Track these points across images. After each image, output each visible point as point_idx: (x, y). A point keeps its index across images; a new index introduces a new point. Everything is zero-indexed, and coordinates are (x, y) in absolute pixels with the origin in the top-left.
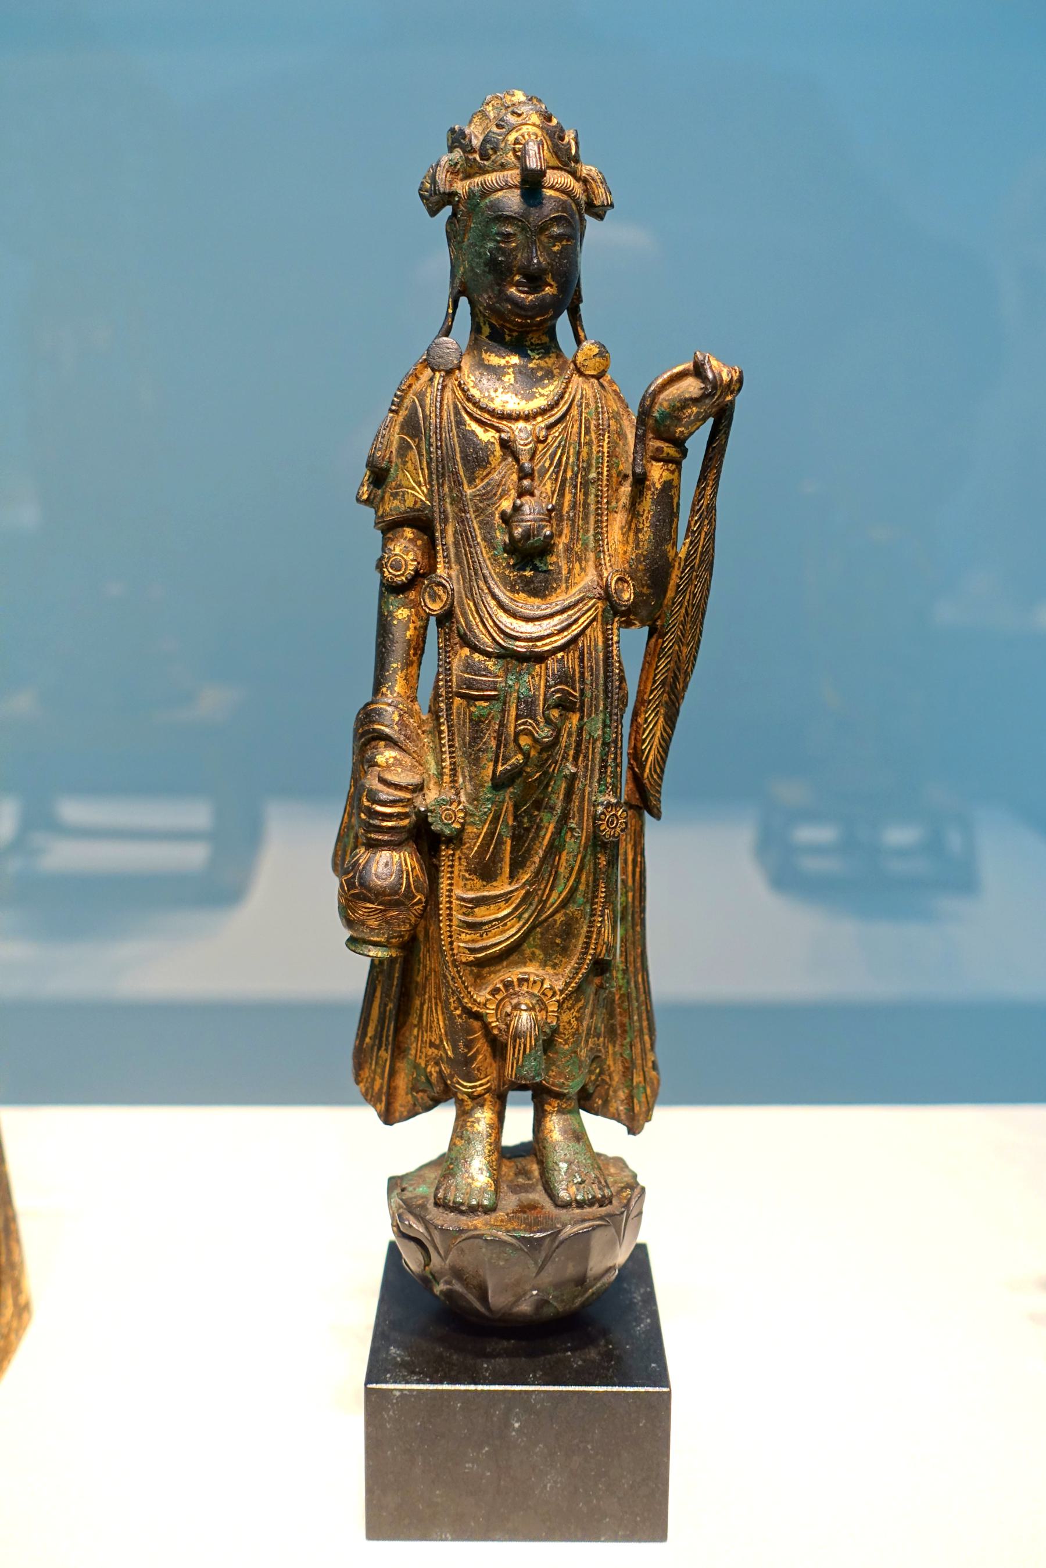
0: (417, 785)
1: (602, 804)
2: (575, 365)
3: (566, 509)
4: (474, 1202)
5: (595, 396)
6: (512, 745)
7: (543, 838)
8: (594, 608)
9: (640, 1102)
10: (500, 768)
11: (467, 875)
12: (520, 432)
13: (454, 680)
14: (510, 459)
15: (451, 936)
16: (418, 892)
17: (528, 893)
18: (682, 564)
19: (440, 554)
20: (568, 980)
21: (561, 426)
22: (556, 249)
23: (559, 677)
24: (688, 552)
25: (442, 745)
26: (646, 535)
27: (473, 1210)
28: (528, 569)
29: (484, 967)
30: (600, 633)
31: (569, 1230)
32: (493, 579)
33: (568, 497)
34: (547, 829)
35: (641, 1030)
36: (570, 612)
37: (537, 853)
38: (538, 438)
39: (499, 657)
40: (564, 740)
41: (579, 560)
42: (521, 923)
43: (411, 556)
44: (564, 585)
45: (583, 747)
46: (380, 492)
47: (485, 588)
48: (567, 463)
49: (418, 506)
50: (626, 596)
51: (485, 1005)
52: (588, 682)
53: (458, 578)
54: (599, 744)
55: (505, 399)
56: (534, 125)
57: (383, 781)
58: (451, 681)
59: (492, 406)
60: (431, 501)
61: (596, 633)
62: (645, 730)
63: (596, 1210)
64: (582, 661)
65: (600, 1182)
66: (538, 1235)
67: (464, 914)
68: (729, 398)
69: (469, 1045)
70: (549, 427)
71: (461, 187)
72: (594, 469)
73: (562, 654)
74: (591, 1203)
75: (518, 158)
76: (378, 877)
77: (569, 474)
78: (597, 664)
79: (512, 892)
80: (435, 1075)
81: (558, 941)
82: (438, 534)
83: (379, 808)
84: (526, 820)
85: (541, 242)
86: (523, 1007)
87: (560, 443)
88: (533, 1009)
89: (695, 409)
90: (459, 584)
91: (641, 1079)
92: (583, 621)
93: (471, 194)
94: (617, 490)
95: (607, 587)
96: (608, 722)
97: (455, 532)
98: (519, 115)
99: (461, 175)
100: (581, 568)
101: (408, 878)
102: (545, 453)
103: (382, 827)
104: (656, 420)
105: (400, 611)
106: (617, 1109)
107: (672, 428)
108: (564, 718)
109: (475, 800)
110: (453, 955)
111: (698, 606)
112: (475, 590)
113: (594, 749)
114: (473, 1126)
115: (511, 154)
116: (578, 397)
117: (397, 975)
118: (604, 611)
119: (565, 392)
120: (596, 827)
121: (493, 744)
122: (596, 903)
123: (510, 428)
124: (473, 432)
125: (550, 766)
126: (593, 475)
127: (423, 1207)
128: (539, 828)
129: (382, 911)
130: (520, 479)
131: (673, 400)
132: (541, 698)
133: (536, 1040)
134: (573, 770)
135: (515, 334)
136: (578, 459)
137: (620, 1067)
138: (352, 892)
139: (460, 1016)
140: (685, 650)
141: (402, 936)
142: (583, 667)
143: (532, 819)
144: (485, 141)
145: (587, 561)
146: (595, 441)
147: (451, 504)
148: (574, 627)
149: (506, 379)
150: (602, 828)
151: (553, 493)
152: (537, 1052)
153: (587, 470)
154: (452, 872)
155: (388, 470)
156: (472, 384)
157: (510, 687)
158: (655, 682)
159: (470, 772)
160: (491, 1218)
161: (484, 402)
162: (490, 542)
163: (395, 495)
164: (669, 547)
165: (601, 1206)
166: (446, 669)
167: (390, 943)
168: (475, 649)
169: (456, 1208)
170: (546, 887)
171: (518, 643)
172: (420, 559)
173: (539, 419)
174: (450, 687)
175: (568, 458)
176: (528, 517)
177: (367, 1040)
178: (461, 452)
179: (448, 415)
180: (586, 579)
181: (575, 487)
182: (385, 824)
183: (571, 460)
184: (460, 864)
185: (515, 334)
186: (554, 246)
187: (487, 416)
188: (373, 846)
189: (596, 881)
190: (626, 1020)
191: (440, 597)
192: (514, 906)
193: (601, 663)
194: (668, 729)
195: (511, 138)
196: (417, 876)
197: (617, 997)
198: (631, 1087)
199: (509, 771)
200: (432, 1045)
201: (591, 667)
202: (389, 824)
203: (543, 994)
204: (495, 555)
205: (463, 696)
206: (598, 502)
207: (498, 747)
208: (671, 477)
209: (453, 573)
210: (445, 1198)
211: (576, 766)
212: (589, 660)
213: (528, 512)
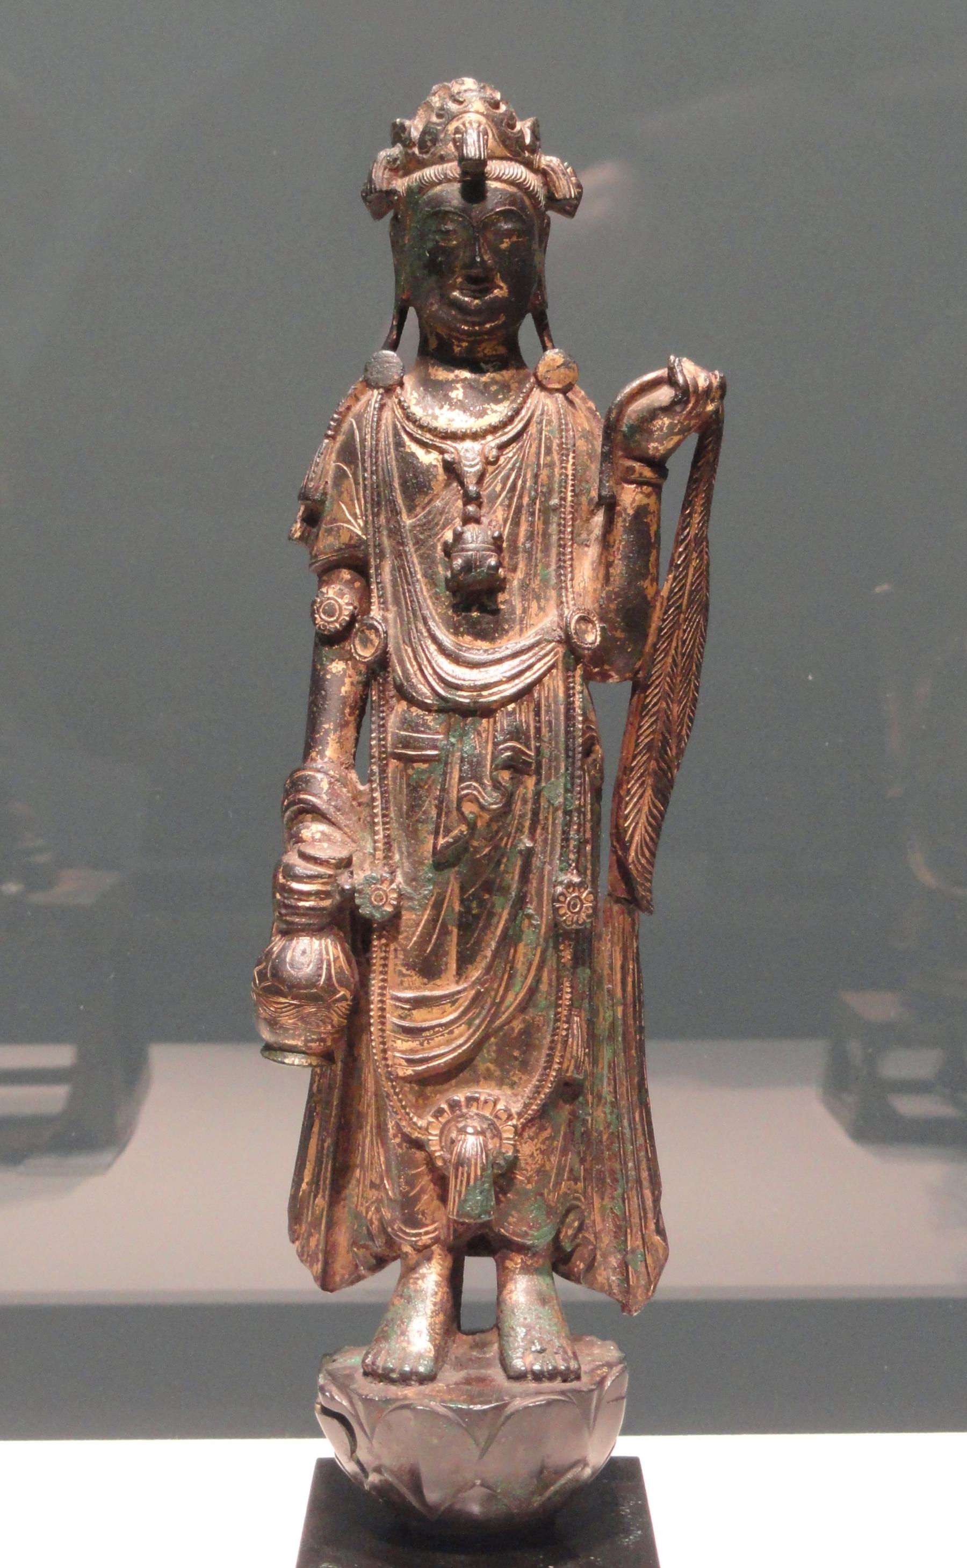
0: (341, 860)
1: (561, 883)
2: (536, 377)
3: (522, 538)
4: (407, 1369)
5: (558, 412)
6: (455, 813)
7: (497, 927)
8: (552, 654)
9: (636, 1271)
10: (441, 841)
11: (404, 971)
12: (469, 454)
13: (389, 738)
14: (455, 484)
15: (384, 1043)
16: (341, 985)
17: (478, 994)
18: (665, 604)
19: (375, 594)
20: (527, 1101)
21: (514, 447)
22: (504, 246)
23: (510, 733)
24: (671, 590)
25: (374, 816)
26: (619, 569)
27: (404, 1379)
28: (474, 608)
29: (429, 1084)
30: (561, 683)
31: (518, 1403)
32: (434, 621)
33: (523, 529)
34: (500, 917)
35: (639, 1181)
36: (524, 657)
37: (489, 945)
38: (487, 458)
39: (440, 711)
40: (518, 808)
41: (538, 598)
42: (471, 1030)
43: (347, 598)
44: (518, 627)
45: (541, 817)
46: (315, 530)
47: (424, 630)
48: (523, 488)
49: (353, 542)
50: (590, 638)
51: (427, 1129)
52: (546, 739)
53: (395, 622)
54: (560, 814)
55: (448, 418)
56: (477, 112)
57: (304, 856)
58: (384, 739)
59: (434, 424)
60: (366, 534)
61: (556, 683)
62: (627, 803)
63: (558, 1385)
64: (538, 714)
65: (565, 1352)
66: (478, 1407)
67: (400, 1017)
68: (710, 408)
69: (411, 1182)
70: (502, 447)
71: (401, 184)
72: (556, 495)
73: (513, 705)
74: (552, 1375)
75: (457, 147)
76: (292, 966)
77: (526, 500)
78: (557, 719)
79: (459, 992)
80: (376, 1223)
81: (516, 1054)
82: (372, 571)
83: (295, 886)
84: (474, 905)
85: (485, 239)
86: (470, 1130)
87: (514, 465)
88: (482, 1133)
89: (667, 421)
90: (396, 627)
91: (639, 1242)
92: (540, 668)
93: (410, 190)
94: (588, 520)
95: (566, 629)
96: (569, 786)
97: (393, 569)
98: (461, 103)
99: (401, 173)
100: (540, 608)
101: (329, 970)
102: (497, 475)
103: (298, 907)
104: (624, 436)
105: (334, 664)
106: (608, 1279)
107: (644, 443)
108: (516, 782)
109: (414, 880)
110: (387, 1066)
111: (690, 656)
112: (414, 633)
113: (554, 819)
114: (416, 1283)
115: (451, 144)
116: (538, 413)
117: (335, 1103)
118: (565, 656)
119: (522, 408)
120: (556, 910)
121: (434, 813)
122: (560, 1006)
123: (455, 448)
124: (413, 454)
125: (502, 839)
126: (555, 501)
127: (350, 1377)
128: (491, 915)
129: (297, 1006)
130: (465, 504)
131: (642, 411)
132: (489, 757)
133: (483, 1169)
134: (529, 844)
135: (465, 344)
136: (536, 483)
137: (610, 1225)
138: (264, 984)
139: (400, 1145)
140: (676, 709)
141: (323, 1040)
142: (539, 722)
143: (482, 904)
144: (424, 133)
145: (547, 600)
146: (557, 463)
147: (389, 537)
148: (528, 674)
149: (453, 394)
150: (562, 912)
151: (505, 521)
152: (484, 1183)
153: (548, 495)
154: (385, 966)
155: (323, 502)
156: (414, 401)
157: (453, 745)
158: (637, 745)
159: (408, 847)
160: (427, 1388)
161: (426, 420)
162: (431, 579)
163: (329, 531)
164: (646, 583)
165: (565, 1381)
166: (380, 726)
167: (310, 1048)
168: (412, 701)
169: (384, 1377)
170: (500, 985)
171: (459, 693)
172: (356, 604)
173: (489, 438)
174: (384, 746)
175: (524, 482)
176: (472, 546)
177: (304, 1186)
178: (400, 477)
179: (385, 435)
180: (545, 621)
181: (533, 514)
182: (301, 904)
183: (528, 484)
184: (396, 957)
185: (465, 344)
186: (502, 242)
187: (428, 436)
188: (290, 932)
189: (559, 978)
190: (617, 1166)
191: (371, 641)
192: (462, 1009)
193: (562, 718)
194: (659, 805)
195: (451, 128)
196: (341, 967)
197: (605, 1137)
198: (624, 1252)
199: (452, 844)
200: (373, 1185)
201: (550, 722)
202: (307, 904)
203: (497, 1117)
204: (436, 593)
205: (399, 757)
206: (560, 532)
207: (439, 815)
208: (646, 501)
209: (390, 616)
210: (373, 1363)
211: (532, 837)
212: (547, 712)
213: (470, 539)
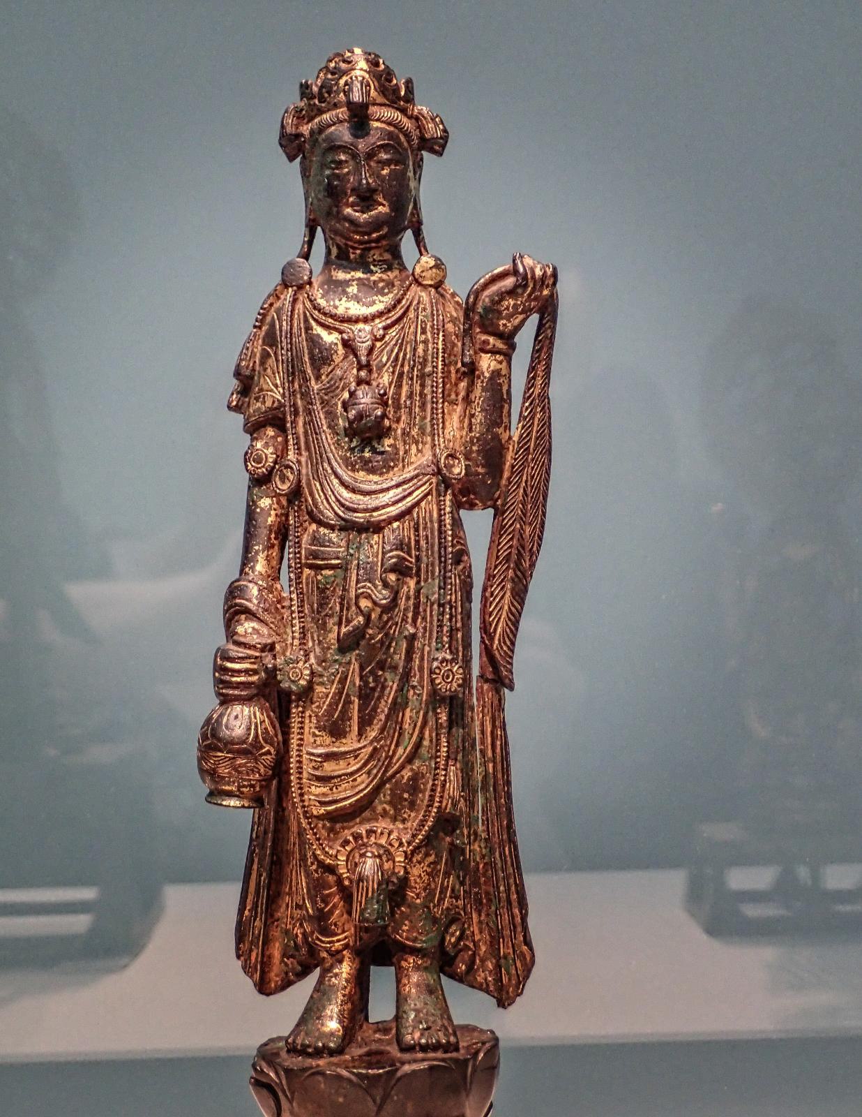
0: (265, 645)
1: (437, 659)
5: (431, 303)
10: (344, 630)
11: (317, 733)
12: (362, 333)
13: (303, 553)
14: (351, 357)
15: (301, 788)
16: (266, 742)
17: (375, 749)
18: (516, 446)
24: (521, 436)
26: (479, 417)
29: (338, 822)
30: (435, 506)
31: (407, 1068)
33: (405, 389)
34: (391, 688)
35: (509, 902)
36: (406, 487)
38: (375, 336)
39: (341, 529)
40: (402, 603)
44: (401, 465)
45: (421, 610)
46: (247, 400)
47: (329, 469)
48: (404, 359)
49: (276, 405)
50: (456, 470)
51: (336, 856)
54: (435, 607)
56: (361, 69)
58: (299, 552)
59: (334, 311)
61: (430, 506)
62: (491, 603)
64: (417, 530)
66: (375, 1071)
68: (546, 292)
69: (325, 900)
70: (386, 328)
72: (430, 364)
73: (397, 523)
74: (436, 1047)
76: (227, 727)
77: (406, 369)
78: (432, 533)
79: (360, 749)
80: (300, 936)
81: (406, 795)
82: (289, 425)
83: (229, 665)
84: (371, 680)
86: (369, 854)
88: (380, 856)
89: (512, 302)
91: (511, 951)
95: (437, 464)
96: (442, 584)
97: (305, 423)
98: (349, 62)
99: (305, 121)
100: (419, 451)
103: (231, 682)
105: (262, 500)
106: (486, 979)
110: (304, 807)
115: (342, 94)
116: (415, 302)
118: (438, 485)
119: (403, 298)
120: (432, 681)
122: (439, 757)
123: (350, 329)
124: (318, 336)
125: (390, 628)
126: (428, 369)
127: (277, 1054)
128: (384, 688)
134: (412, 630)
135: (358, 252)
136: (414, 355)
138: (205, 743)
139: (316, 871)
141: (252, 786)
142: (418, 535)
147: (301, 399)
148: (409, 499)
149: (349, 290)
150: (437, 681)
151: (390, 384)
152: (380, 895)
156: (320, 296)
157: (352, 555)
158: (498, 557)
159: (318, 636)
163: (257, 399)
164: (501, 430)
167: (242, 793)
168: (320, 523)
170: (391, 743)
171: (356, 515)
173: (377, 321)
175: (405, 355)
176: (363, 401)
177: (247, 913)
180: (420, 458)
181: (412, 379)
182: (234, 679)
183: (408, 356)
184: (310, 722)
185: (358, 252)
186: (383, 169)
187: (330, 320)
190: (491, 890)
193: (436, 533)
194: (516, 604)
195: (342, 82)
196: (266, 729)
197: (481, 866)
198: (498, 958)
201: (427, 536)
202: (238, 679)
203: (391, 844)
205: (311, 567)
207: (342, 610)
208: (499, 366)
210: (294, 1042)
212: (425, 528)
213: (362, 396)
